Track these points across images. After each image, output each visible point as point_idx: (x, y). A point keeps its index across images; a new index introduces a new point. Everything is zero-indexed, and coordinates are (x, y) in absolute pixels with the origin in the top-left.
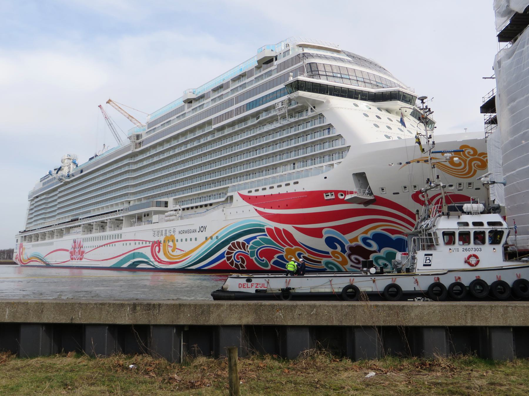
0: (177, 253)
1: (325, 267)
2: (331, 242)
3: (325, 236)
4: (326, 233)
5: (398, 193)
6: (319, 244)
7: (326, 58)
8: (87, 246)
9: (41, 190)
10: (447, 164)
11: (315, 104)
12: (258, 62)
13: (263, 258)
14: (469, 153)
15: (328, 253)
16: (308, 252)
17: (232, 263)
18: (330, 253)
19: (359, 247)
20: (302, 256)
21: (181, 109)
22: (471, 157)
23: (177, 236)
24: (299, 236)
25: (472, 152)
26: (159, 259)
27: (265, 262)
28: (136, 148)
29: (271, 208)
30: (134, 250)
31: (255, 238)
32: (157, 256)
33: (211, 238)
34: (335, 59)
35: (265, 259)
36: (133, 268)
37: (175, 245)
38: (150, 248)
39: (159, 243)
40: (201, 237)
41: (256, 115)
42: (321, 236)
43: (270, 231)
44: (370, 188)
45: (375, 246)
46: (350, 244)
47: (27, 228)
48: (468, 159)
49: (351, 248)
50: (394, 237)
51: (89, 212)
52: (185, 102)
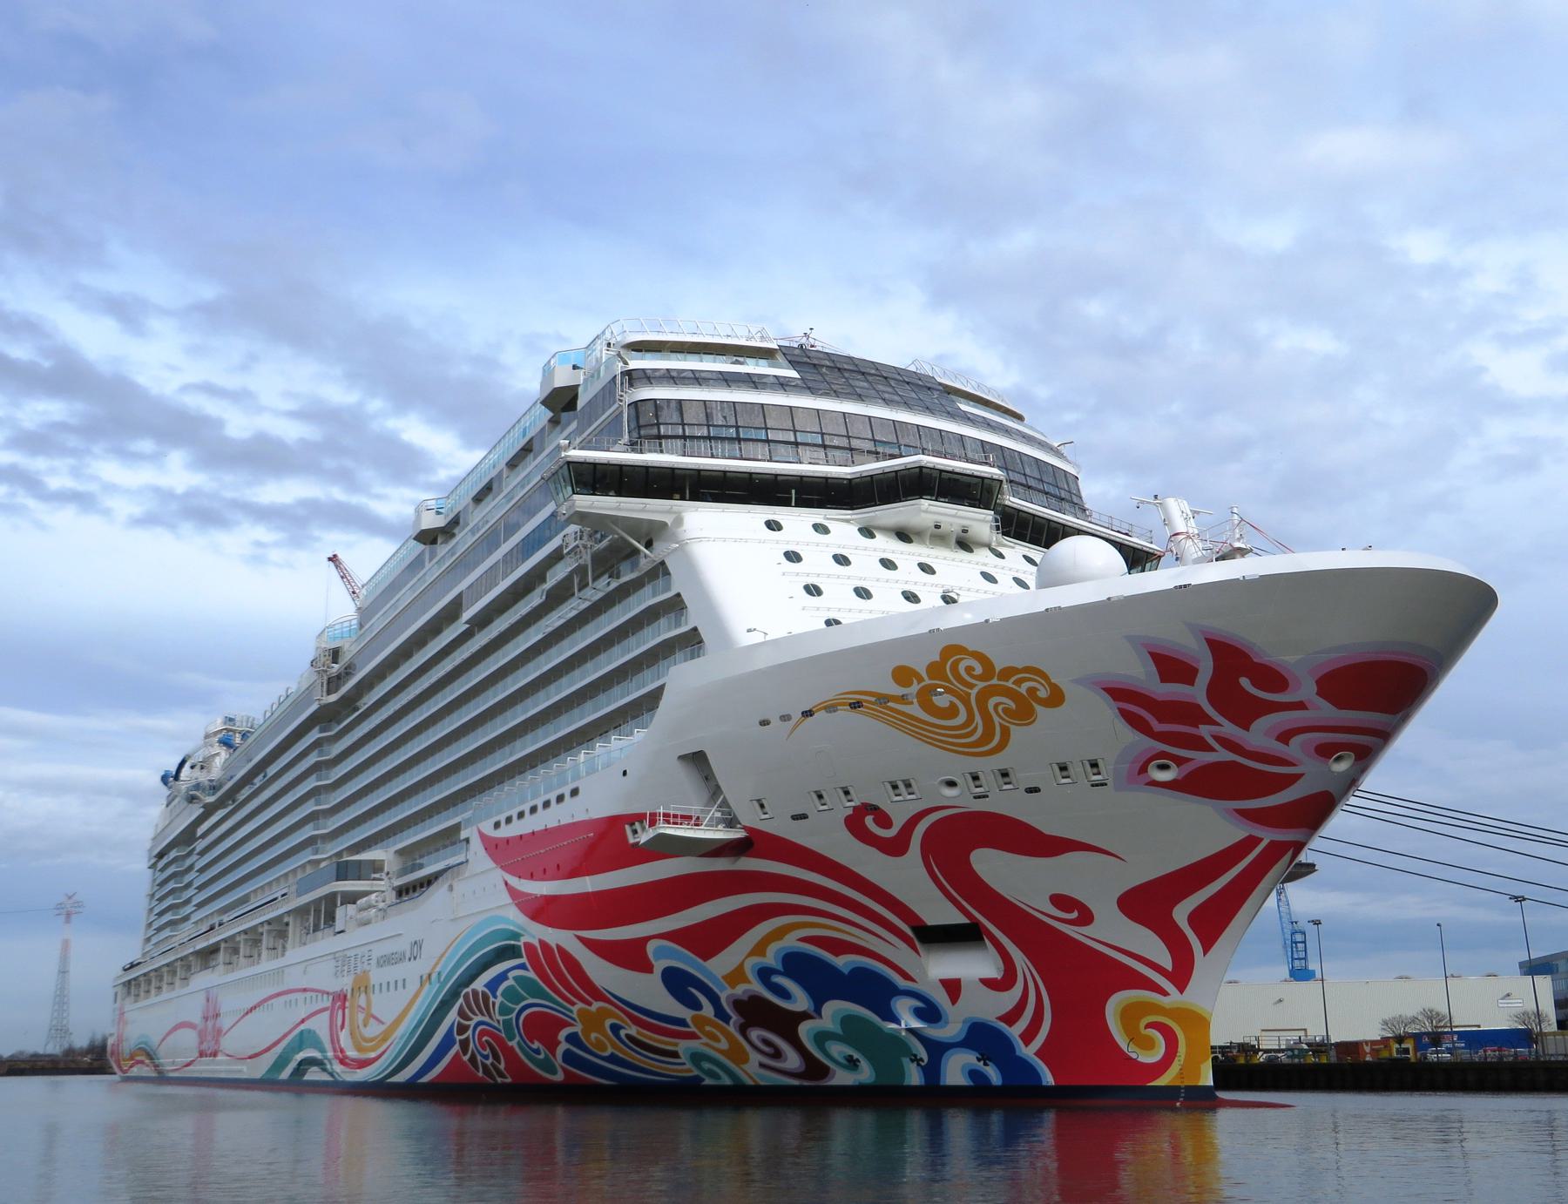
0: (373, 1030)
1: (696, 1072)
2: (677, 982)
3: (659, 966)
4: (660, 953)
5: (804, 817)
7: (697, 379)
10: (915, 710)
11: (651, 533)
13: (536, 1045)
14: (969, 669)
15: (682, 1022)
17: (473, 1059)
18: (689, 1021)
19: (755, 1000)
20: (622, 1033)
21: (416, 565)
22: (981, 685)
23: (377, 976)
24: (599, 971)
25: (979, 670)
27: (542, 1056)
28: (329, 693)
29: (532, 877)
30: (303, 1021)
31: (502, 977)
34: (727, 380)
36: (297, 1084)
38: (326, 1015)
39: (341, 998)
40: (412, 971)
42: (647, 967)
44: (725, 803)
46: (729, 991)
47: (144, 955)
48: (974, 692)
49: (738, 1004)
50: (843, 962)
51: (244, 900)
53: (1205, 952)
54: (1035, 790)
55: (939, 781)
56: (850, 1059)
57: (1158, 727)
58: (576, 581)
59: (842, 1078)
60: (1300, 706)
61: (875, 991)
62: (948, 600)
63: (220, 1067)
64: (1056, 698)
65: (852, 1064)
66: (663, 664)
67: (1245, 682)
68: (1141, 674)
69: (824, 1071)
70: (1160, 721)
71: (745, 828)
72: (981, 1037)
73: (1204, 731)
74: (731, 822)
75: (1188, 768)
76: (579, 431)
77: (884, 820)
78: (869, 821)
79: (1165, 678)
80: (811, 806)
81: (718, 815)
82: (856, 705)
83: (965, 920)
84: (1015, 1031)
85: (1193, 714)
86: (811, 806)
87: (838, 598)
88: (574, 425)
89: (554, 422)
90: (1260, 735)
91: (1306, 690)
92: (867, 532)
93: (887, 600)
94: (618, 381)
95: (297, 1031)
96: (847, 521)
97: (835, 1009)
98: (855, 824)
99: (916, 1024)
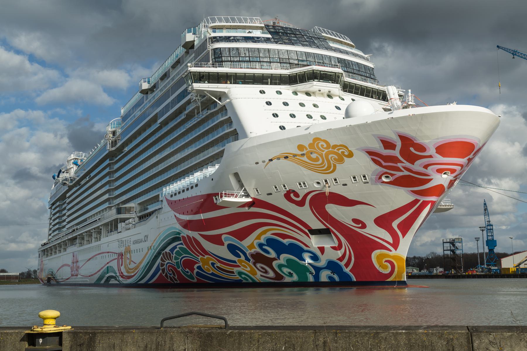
0: (132, 266)
1: (240, 278)
2: (232, 249)
3: (226, 243)
4: (226, 239)
6: (223, 252)
11: (221, 96)
13: (187, 270)
14: (322, 146)
17: (166, 275)
19: (258, 254)
22: (326, 151)
23: (133, 247)
24: (207, 245)
25: (325, 146)
27: (189, 274)
31: (175, 247)
36: (107, 284)
38: (116, 260)
39: (121, 255)
42: (223, 244)
44: (245, 190)
46: (249, 251)
47: (49, 240)
48: (324, 153)
49: (252, 255)
50: (286, 241)
51: (85, 220)
53: (403, 237)
54: (346, 185)
56: (290, 273)
58: (196, 111)
59: (287, 279)
60: (430, 156)
61: (297, 251)
62: (323, 118)
63: (79, 279)
64: (351, 155)
65: (291, 275)
66: (226, 141)
67: (412, 149)
68: (377, 147)
69: (282, 277)
70: (385, 162)
71: (252, 198)
72: (332, 266)
73: (399, 165)
74: (248, 196)
76: (195, 58)
78: (292, 195)
79: (386, 148)
81: (243, 194)
82: (286, 157)
83: (325, 227)
84: (342, 264)
85: (394, 159)
87: (284, 119)
88: (193, 55)
89: (187, 53)
90: (418, 166)
91: (432, 151)
92: (295, 93)
93: (301, 119)
94: (208, 40)
95: (106, 266)
96: (288, 89)
97: (284, 257)
98: (287, 196)
99: (311, 261)
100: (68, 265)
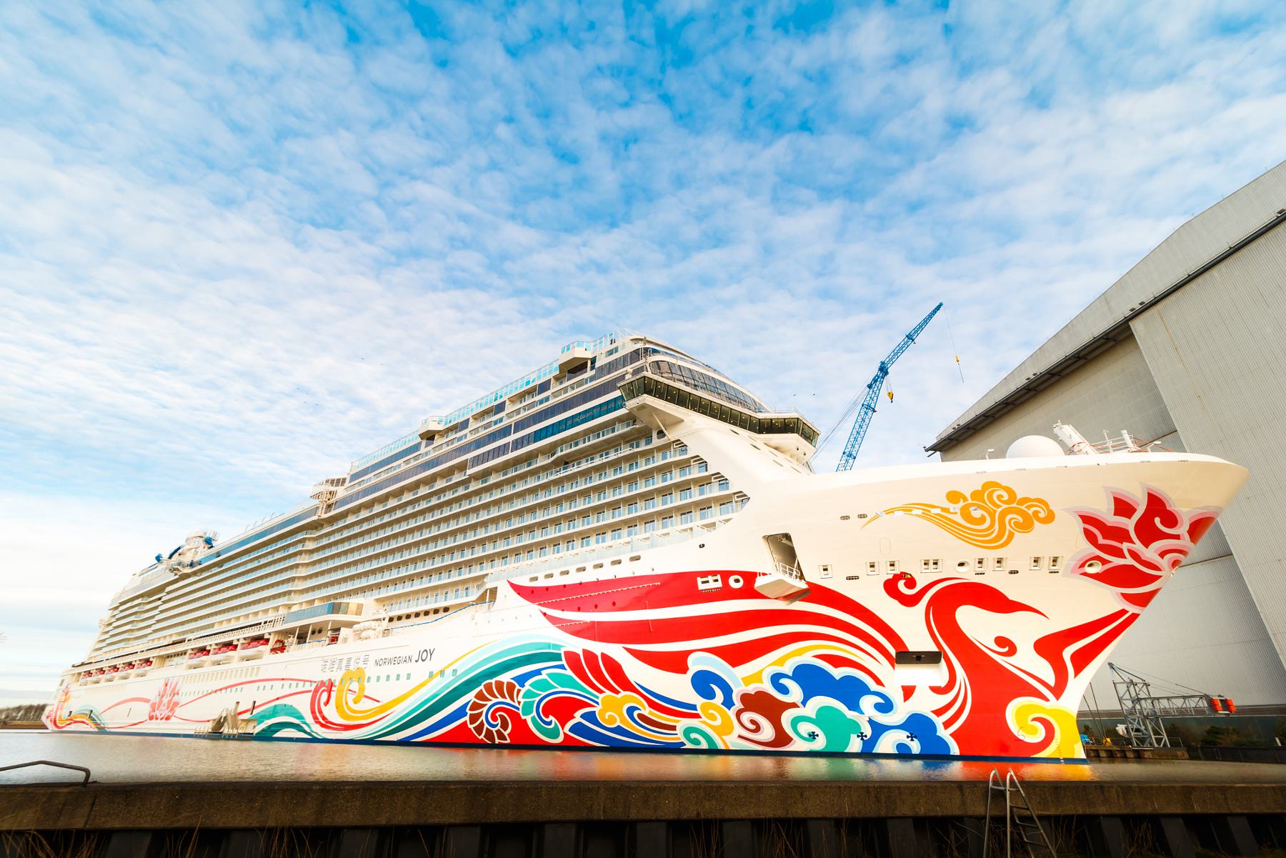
0: (366, 705)
1: (683, 740)
2: (704, 683)
4: (697, 662)
6: (677, 687)
8: (187, 691)
9: (135, 589)
10: (958, 518)
12: (561, 366)
13: (551, 718)
14: (999, 497)
15: (694, 707)
16: (652, 705)
17: (479, 729)
19: (761, 695)
20: (636, 713)
21: (416, 448)
22: (1005, 506)
23: (371, 670)
24: (636, 671)
25: (1006, 497)
26: (324, 718)
29: (579, 610)
31: (538, 672)
32: (320, 712)
33: (442, 673)
35: (554, 720)
37: (362, 689)
40: (420, 671)
41: (551, 450)
42: (683, 669)
43: (572, 659)
45: (796, 693)
48: (999, 510)
49: (745, 698)
50: (838, 673)
51: (212, 625)
52: (422, 436)
53: (1077, 673)
55: (956, 561)
57: (1101, 541)
60: (1177, 537)
63: (173, 726)
67: (1157, 520)
70: (1104, 538)
72: (917, 725)
75: (1108, 566)
77: (911, 583)
80: (862, 571)
84: (939, 721)
85: (1122, 535)
86: (862, 571)
90: (1150, 553)
91: (1182, 529)
97: (819, 701)
100: (147, 701)
